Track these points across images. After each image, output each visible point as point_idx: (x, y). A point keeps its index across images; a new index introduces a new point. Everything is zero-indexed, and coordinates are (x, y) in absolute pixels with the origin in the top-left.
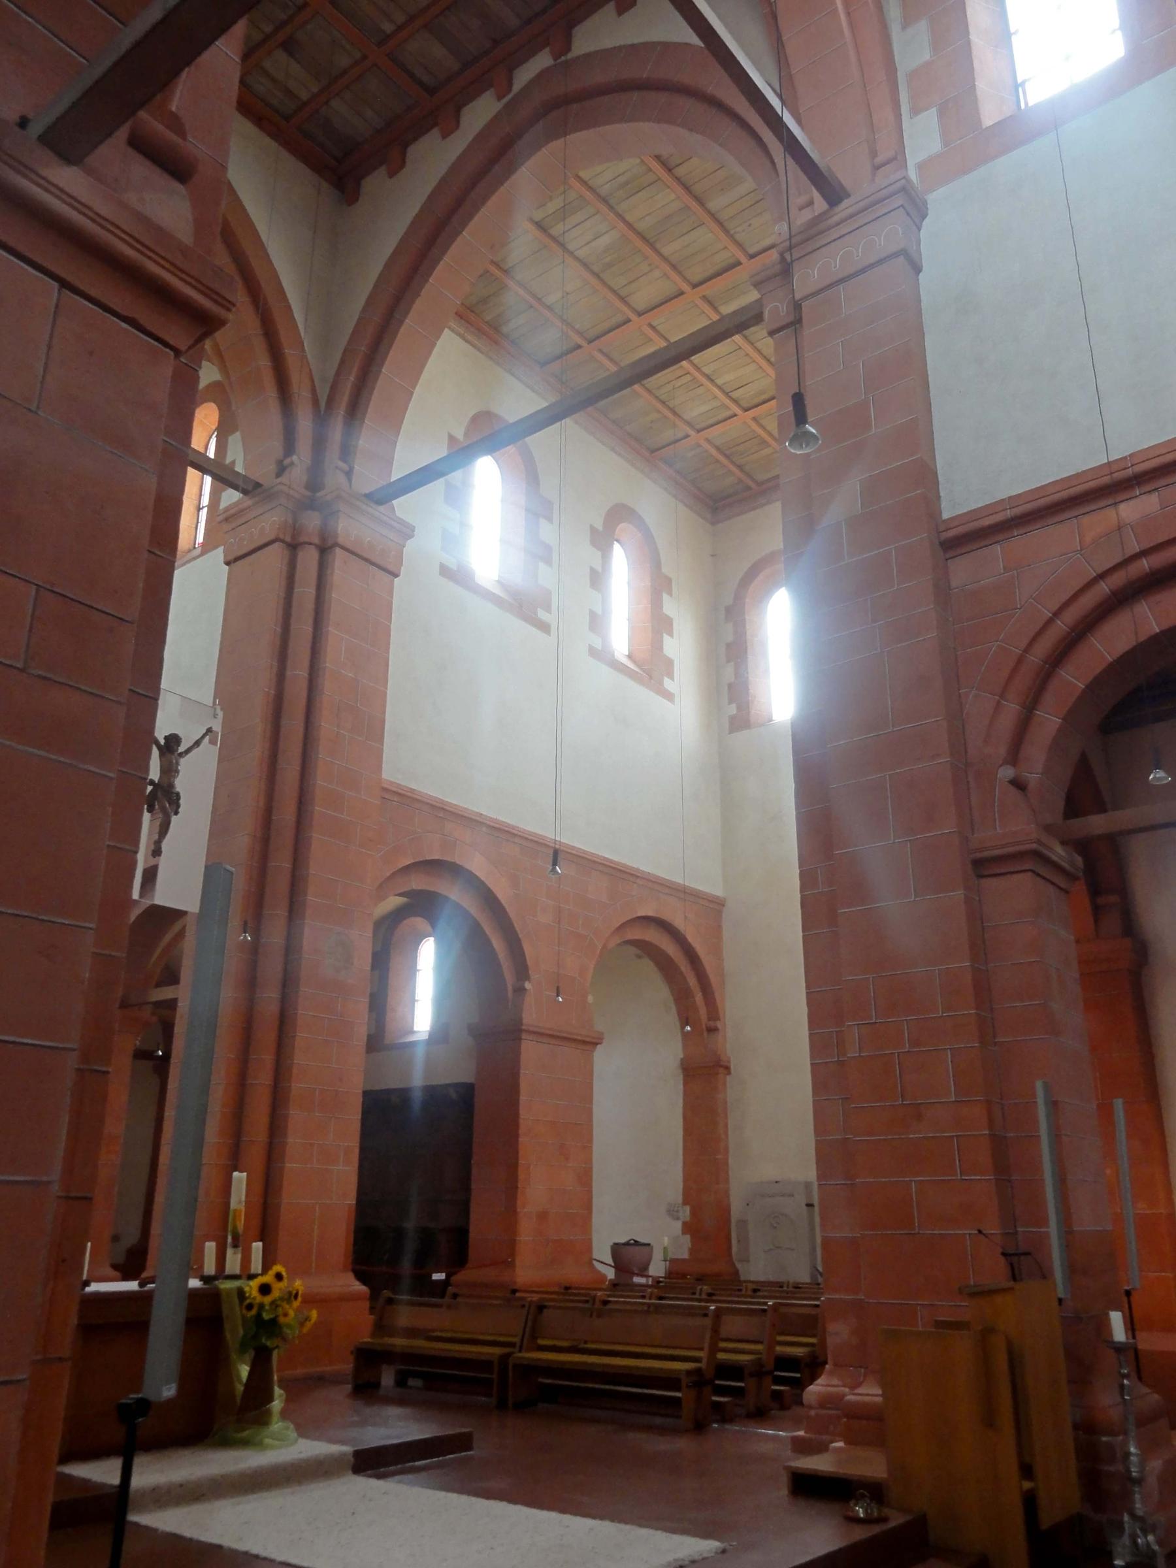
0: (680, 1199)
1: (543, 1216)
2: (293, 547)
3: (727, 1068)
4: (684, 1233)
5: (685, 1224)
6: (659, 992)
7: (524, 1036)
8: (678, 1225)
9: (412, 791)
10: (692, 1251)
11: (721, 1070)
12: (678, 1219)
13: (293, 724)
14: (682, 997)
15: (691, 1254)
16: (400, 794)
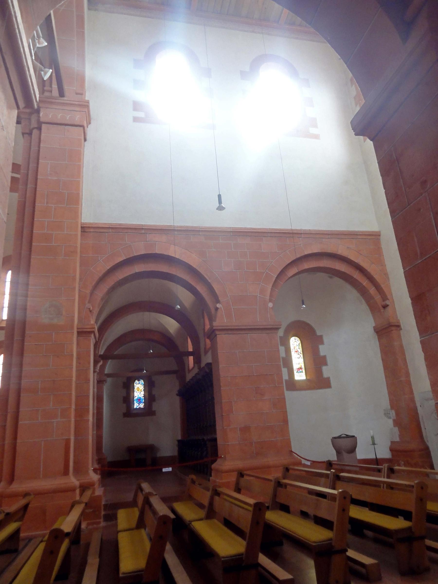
0: (389, 407)
1: (245, 430)
2: (30, 134)
3: (398, 326)
4: (394, 426)
5: (394, 421)
6: (352, 294)
7: (217, 333)
8: (390, 422)
9: (120, 224)
10: (401, 436)
11: (393, 328)
12: (390, 418)
13: (28, 210)
14: (363, 292)
15: (400, 438)
16: (112, 228)
